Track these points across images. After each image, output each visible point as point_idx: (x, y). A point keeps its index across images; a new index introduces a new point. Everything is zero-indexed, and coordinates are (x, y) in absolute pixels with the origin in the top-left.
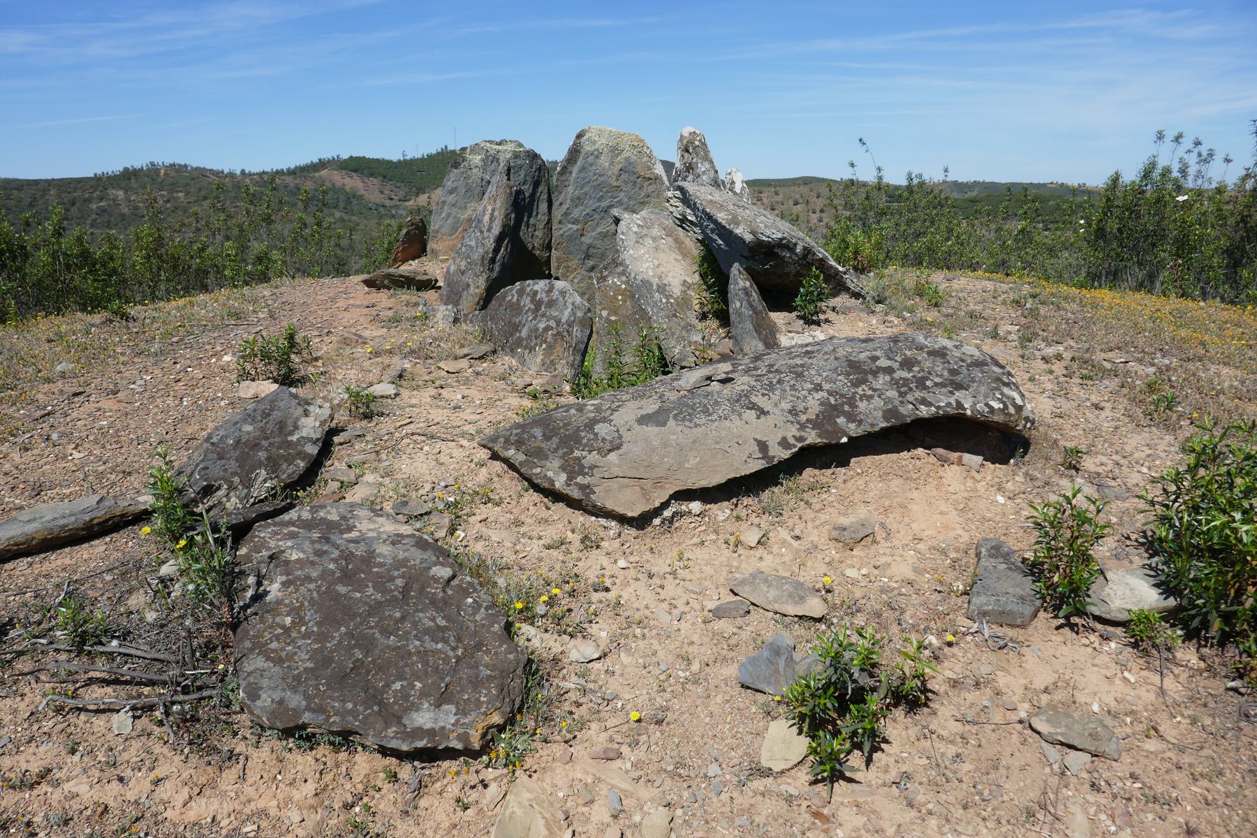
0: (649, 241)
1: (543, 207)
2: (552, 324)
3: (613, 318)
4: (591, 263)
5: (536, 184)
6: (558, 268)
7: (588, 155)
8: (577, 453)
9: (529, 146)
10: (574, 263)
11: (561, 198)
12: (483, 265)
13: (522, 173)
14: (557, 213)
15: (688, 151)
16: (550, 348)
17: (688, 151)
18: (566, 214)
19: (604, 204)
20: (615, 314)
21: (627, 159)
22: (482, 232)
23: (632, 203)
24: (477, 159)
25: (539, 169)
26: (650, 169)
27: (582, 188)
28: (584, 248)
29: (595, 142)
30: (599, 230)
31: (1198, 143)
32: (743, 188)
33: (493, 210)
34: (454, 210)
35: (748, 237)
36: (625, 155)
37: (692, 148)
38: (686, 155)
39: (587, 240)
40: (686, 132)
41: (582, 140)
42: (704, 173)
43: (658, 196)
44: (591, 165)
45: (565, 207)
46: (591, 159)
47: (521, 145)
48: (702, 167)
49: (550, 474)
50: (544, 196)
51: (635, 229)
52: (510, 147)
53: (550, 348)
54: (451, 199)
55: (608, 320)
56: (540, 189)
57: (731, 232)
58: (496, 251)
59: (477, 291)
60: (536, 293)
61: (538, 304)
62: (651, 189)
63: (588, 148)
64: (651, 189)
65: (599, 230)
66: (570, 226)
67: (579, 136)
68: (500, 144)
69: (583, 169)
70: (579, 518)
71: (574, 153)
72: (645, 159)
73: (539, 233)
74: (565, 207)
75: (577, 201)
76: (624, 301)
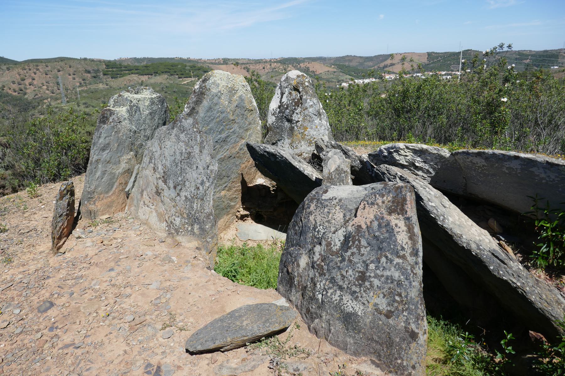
17: (296, 89)
19: (223, 135)
21: (240, 97)
27: (208, 125)
29: (218, 85)
36: (240, 93)
38: (294, 93)
44: (216, 104)
46: (215, 101)
54: (105, 155)
69: (210, 109)
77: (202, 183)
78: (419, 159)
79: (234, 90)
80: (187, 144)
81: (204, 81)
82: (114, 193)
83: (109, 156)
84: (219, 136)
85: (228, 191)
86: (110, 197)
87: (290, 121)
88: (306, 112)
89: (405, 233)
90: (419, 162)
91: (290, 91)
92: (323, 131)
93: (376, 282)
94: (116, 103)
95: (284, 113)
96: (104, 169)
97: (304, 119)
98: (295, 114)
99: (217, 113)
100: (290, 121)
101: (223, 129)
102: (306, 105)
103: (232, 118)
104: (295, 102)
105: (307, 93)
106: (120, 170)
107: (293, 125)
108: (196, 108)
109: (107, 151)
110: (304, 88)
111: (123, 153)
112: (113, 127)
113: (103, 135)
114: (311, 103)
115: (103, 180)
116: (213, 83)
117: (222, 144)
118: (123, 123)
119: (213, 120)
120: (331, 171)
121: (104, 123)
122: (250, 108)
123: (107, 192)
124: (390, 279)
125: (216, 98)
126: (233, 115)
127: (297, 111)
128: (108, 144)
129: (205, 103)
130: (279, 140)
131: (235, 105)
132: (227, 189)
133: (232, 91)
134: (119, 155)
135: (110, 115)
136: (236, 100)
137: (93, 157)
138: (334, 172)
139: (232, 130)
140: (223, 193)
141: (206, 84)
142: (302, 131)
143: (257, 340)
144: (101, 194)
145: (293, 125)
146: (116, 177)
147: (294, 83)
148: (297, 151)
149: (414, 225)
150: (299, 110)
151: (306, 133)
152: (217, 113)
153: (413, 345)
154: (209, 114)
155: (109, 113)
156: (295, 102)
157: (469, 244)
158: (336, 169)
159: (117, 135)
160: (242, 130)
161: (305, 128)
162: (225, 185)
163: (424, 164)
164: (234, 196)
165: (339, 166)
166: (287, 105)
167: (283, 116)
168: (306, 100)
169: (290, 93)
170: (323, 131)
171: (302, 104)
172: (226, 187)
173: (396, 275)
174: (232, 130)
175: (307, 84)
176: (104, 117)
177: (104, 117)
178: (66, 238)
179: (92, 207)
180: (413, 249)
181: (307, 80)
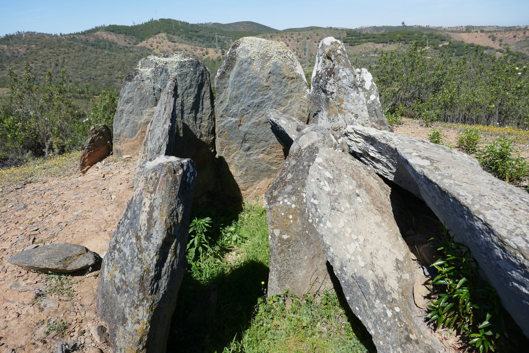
0: (344, 204)
1: (207, 103)
3: (285, 237)
4: (247, 145)
5: (200, 86)
6: (222, 150)
7: (242, 62)
10: (234, 146)
11: (222, 97)
12: (142, 289)
13: (188, 79)
14: (219, 110)
15: (329, 58)
17: (329, 58)
18: (226, 110)
19: (257, 101)
20: (287, 232)
21: (275, 64)
22: (138, 238)
23: (278, 98)
25: (202, 74)
26: (292, 70)
28: (242, 135)
29: (248, 52)
30: (253, 120)
32: (372, 86)
33: (151, 207)
34: (132, 117)
36: (273, 60)
38: (327, 61)
39: (244, 128)
41: (238, 49)
42: (344, 77)
43: (299, 91)
44: (246, 70)
45: (225, 104)
46: (245, 66)
50: (208, 95)
51: (327, 188)
54: (128, 107)
55: (280, 239)
56: (204, 89)
58: (160, 264)
59: (137, 327)
62: (293, 86)
63: (242, 56)
64: (293, 86)
65: (253, 120)
66: (230, 119)
69: (239, 74)
72: (289, 62)
73: (205, 124)
74: (225, 104)
75: (235, 99)
76: (295, 219)
78: (372, 148)
79: (266, 56)
81: (234, 47)
82: (136, 139)
83: (131, 108)
84: (252, 101)
85: (267, 154)
86: (133, 141)
87: (325, 91)
88: (340, 83)
89: (146, 214)
90: (373, 152)
91: (324, 59)
92: (361, 106)
94: (143, 65)
95: (318, 82)
96: (127, 118)
97: (339, 91)
98: (328, 85)
99: (249, 78)
100: (325, 91)
101: (255, 95)
102: (339, 75)
103: (266, 84)
104: (328, 72)
105: (339, 62)
106: (143, 121)
107: (328, 97)
108: (228, 73)
109: (130, 104)
110: (336, 57)
111: (146, 107)
112: (136, 84)
113: (127, 91)
114: (344, 74)
115: (127, 127)
116: (242, 49)
117: (256, 108)
118: (146, 82)
119: (244, 84)
120: (302, 148)
121: (130, 80)
122: (291, 76)
123: (131, 137)
125: (246, 64)
126: (267, 81)
127: (330, 82)
128: (131, 98)
129: (235, 69)
130: (319, 111)
131: (268, 72)
132: (266, 153)
133: (265, 57)
134: (141, 108)
135: (136, 74)
136: (270, 67)
137: (119, 108)
138: (305, 149)
139: (267, 96)
140: (261, 156)
141: (236, 50)
142: (339, 104)
143: (45, 271)
144: (126, 138)
145: (328, 97)
146: (139, 126)
147: (327, 50)
148: (335, 125)
149: (155, 208)
150: (332, 80)
151: (343, 106)
152: (249, 78)
154: (238, 79)
155: (134, 73)
156: (328, 72)
157: (333, 261)
158: (309, 147)
159: (139, 92)
160: (281, 97)
161: (342, 101)
162: (264, 149)
163: (380, 155)
164: (275, 161)
165: (313, 144)
166: (322, 75)
167: (318, 86)
168: (338, 70)
169: (324, 62)
170: (361, 106)
171: (334, 74)
172: (264, 150)
174: (267, 96)
175: (339, 52)
176: (129, 76)
177: (129, 76)
178: (89, 166)
180: (148, 233)
181: (340, 48)
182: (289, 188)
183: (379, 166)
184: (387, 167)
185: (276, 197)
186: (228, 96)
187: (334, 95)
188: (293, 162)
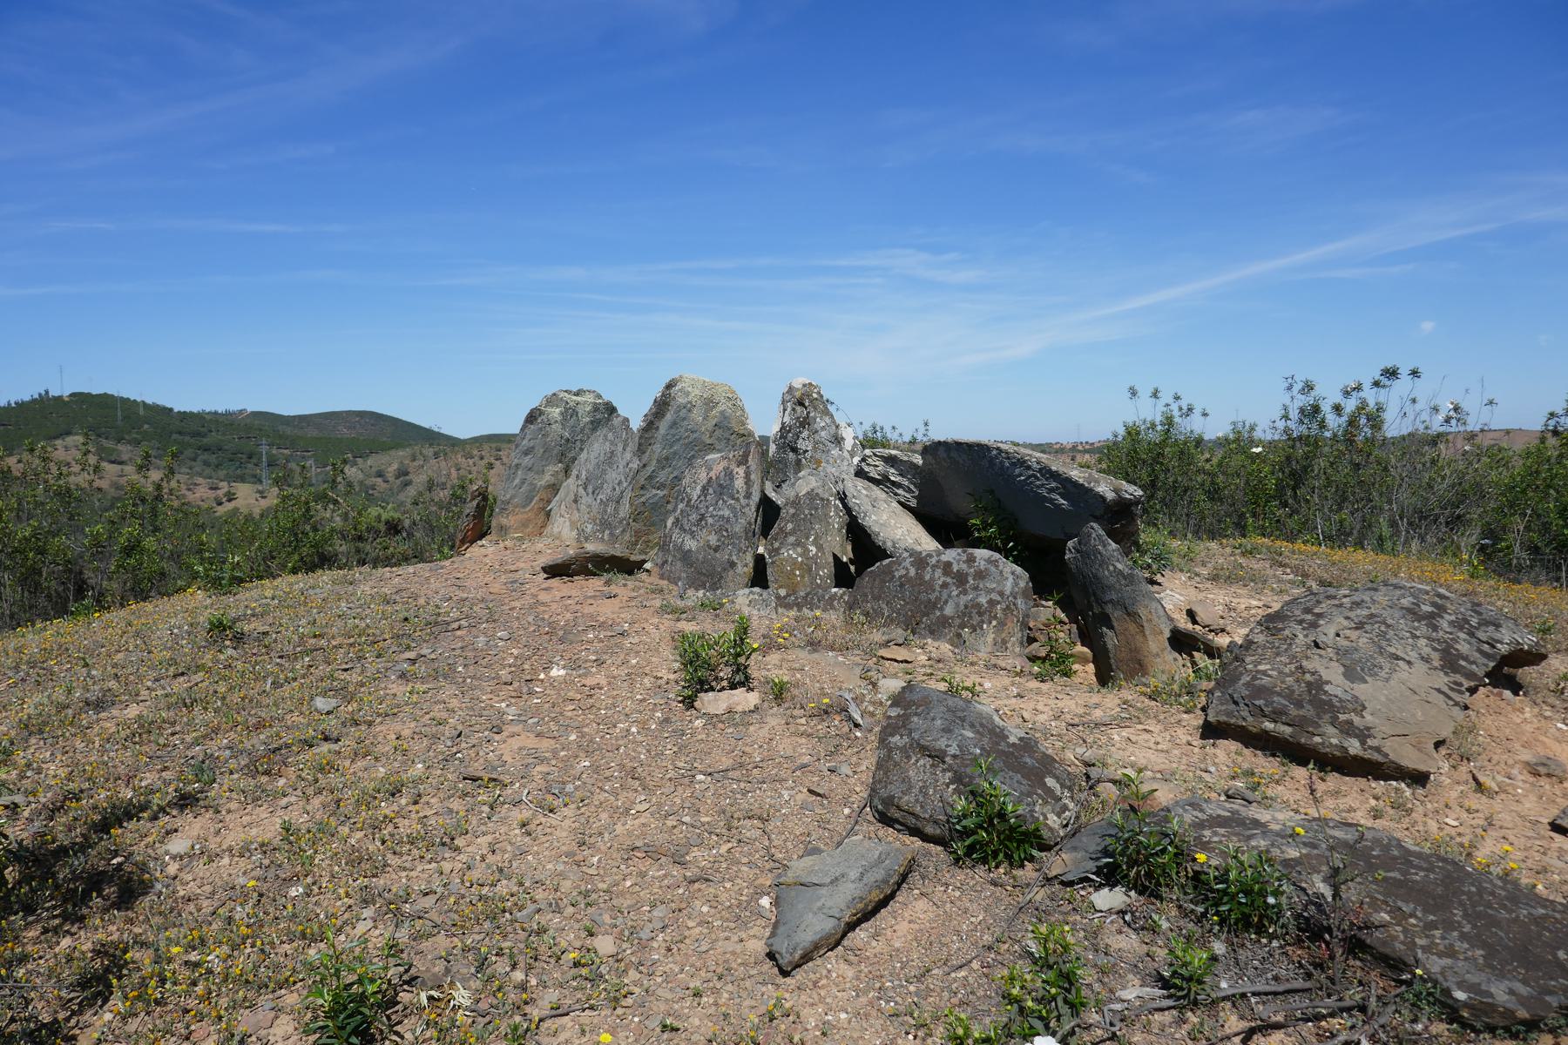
2: (995, 596)
8: (1342, 717)
9: (607, 397)
16: (1002, 624)
17: (801, 404)
18: (650, 478)
21: (722, 413)
24: (555, 412)
29: (688, 394)
31: (1177, 398)
33: (748, 475)
35: (1110, 496)
36: (721, 408)
37: (805, 405)
38: (799, 409)
40: (798, 383)
42: (823, 428)
46: (683, 413)
47: (599, 397)
48: (820, 423)
49: (1334, 741)
52: (590, 398)
53: (1002, 624)
54: (527, 461)
57: (1091, 490)
60: (948, 565)
61: (961, 579)
67: (669, 386)
68: (577, 394)
69: (674, 424)
70: (1379, 786)
71: (662, 405)
76: (802, 576)
77: (620, 483)
80: (612, 443)
93: (710, 520)
100: (795, 450)
124: (722, 517)
129: (669, 417)
147: (798, 394)
150: (805, 434)
153: (731, 573)
173: (727, 513)
179: (504, 521)
182: (792, 539)
183: (900, 491)
184: (909, 491)
185: (779, 549)
186: (656, 456)
187: (808, 455)
188: (792, 511)
